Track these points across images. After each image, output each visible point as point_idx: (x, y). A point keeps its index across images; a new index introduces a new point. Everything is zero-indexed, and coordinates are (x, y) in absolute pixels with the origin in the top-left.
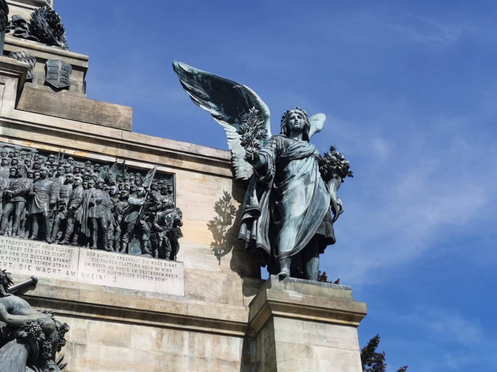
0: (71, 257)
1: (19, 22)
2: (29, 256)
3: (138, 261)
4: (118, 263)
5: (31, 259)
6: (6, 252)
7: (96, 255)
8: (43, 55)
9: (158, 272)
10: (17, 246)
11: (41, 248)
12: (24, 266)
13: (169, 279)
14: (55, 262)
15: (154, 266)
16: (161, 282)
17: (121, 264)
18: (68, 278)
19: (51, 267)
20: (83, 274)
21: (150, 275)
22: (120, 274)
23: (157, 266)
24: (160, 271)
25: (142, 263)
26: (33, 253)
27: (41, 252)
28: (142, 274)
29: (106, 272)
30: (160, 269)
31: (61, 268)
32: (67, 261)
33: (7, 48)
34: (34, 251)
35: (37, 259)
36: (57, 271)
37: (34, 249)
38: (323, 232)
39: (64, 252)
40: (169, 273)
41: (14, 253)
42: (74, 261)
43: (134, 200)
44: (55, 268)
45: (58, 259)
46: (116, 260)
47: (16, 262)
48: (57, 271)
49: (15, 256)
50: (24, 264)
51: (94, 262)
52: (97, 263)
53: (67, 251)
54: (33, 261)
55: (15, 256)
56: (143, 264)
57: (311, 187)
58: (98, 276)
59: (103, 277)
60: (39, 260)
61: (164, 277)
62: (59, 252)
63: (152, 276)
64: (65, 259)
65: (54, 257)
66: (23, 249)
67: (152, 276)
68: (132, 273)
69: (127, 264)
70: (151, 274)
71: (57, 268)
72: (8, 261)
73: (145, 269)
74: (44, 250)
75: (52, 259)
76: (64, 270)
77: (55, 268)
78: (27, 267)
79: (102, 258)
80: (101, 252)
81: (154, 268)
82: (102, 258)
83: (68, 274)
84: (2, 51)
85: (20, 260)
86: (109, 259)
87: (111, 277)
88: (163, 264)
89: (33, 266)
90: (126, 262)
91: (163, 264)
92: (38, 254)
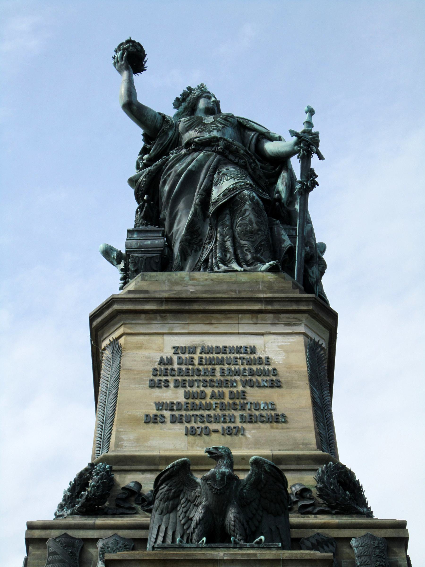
1: (304, 492)
8: (344, 532)
33: (295, 534)
84: (290, 539)
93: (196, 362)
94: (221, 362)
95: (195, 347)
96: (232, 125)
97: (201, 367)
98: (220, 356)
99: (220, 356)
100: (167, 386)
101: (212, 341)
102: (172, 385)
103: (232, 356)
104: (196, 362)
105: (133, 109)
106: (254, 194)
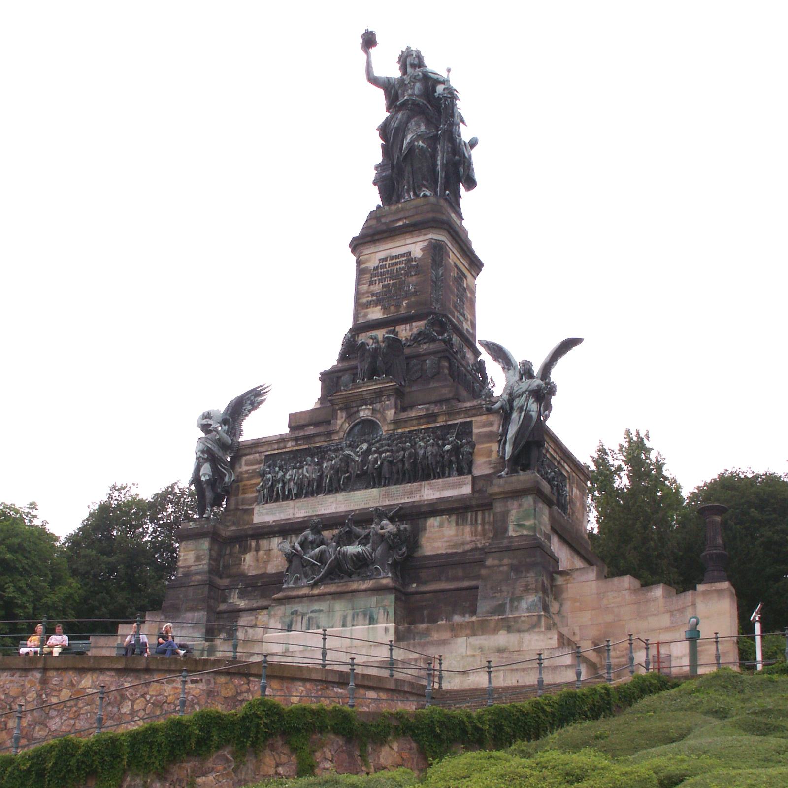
11: (409, 487)
20: (426, 496)
38: (530, 439)
43: (448, 447)
57: (523, 413)
76: (418, 495)
80: (434, 481)
93: (387, 266)
94: (396, 264)
95: (387, 257)
96: (419, 80)
97: (389, 269)
98: (397, 260)
99: (397, 260)
100: (375, 283)
101: (395, 252)
102: (377, 282)
103: (401, 259)
104: (387, 266)
105: (374, 80)
106: (420, 143)
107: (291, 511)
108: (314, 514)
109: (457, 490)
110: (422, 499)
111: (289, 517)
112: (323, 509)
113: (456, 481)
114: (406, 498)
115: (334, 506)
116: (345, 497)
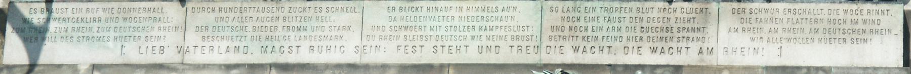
0: (706, 21)
2: (638, 29)
3: (820, 12)
4: (785, 20)
5: (642, 35)
6: (601, 28)
7: (747, 11)
9: (856, 27)
10: (617, 15)
11: (655, 14)
12: (631, 49)
13: (876, 38)
14: (680, 35)
15: (849, 17)
16: (861, 45)
17: (790, 23)
18: (702, 60)
19: (674, 44)
20: (726, 50)
21: (842, 36)
22: (789, 40)
23: (854, 17)
24: (860, 26)
25: (827, 16)
26: (645, 24)
27: (656, 19)
28: (827, 36)
29: (765, 40)
30: (860, 21)
31: (690, 44)
32: (699, 29)
34: (645, 19)
35: (650, 34)
36: (684, 50)
37: (645, 16)
39: (694, 15)
40: (875, 27)
41: (613, 28)
42: (711, 30)
44: (680, 45)
45: (684, 28)
46: (780, 15)
47: (617, 43)
48: (684, 50)
49: (616, 34)
50: (630, 44)
51: (745, 25)
52: (749, 26)
53: (698, 11)
54: (645, 38)
55: (616, 34)
56: (830, 17)
58: (752, 50)
59: (760, 49)
60: (654, 34)
61: (865, 36)
62: (685, 15)
63: (845, 36)
64: (696, 26)
65: (678, 25)
66: (627, 19)
67: (845, 36)
68: (810, 36)
69: (800, 21)
70: (844, 33)
71: (683, 44)
72: (606, 44)
73: (832, 26)
74: (661, 15)
75: (675, 30)
76: (695, 46)
77: (680, 45)
78: (636, 48)
79: (758, 16)
81: (848, 22)
82: (758, 16)
83: (701, 52)
85: (625, 39)
86: (769, 15)
87: (773, 49)
88: (865, 12)
89: (646, 46)
90: (799, 17)
91: (865, 12)
92: (651, 24)
107: (171, 39)
108: (269, 59)
109: (848, 46)
110: (710, 60)
111: (159, 59)
112: (305, 45)
113: (842, 15)
114: (646, 50)
115: (352, 40)
116: (397, 14)
